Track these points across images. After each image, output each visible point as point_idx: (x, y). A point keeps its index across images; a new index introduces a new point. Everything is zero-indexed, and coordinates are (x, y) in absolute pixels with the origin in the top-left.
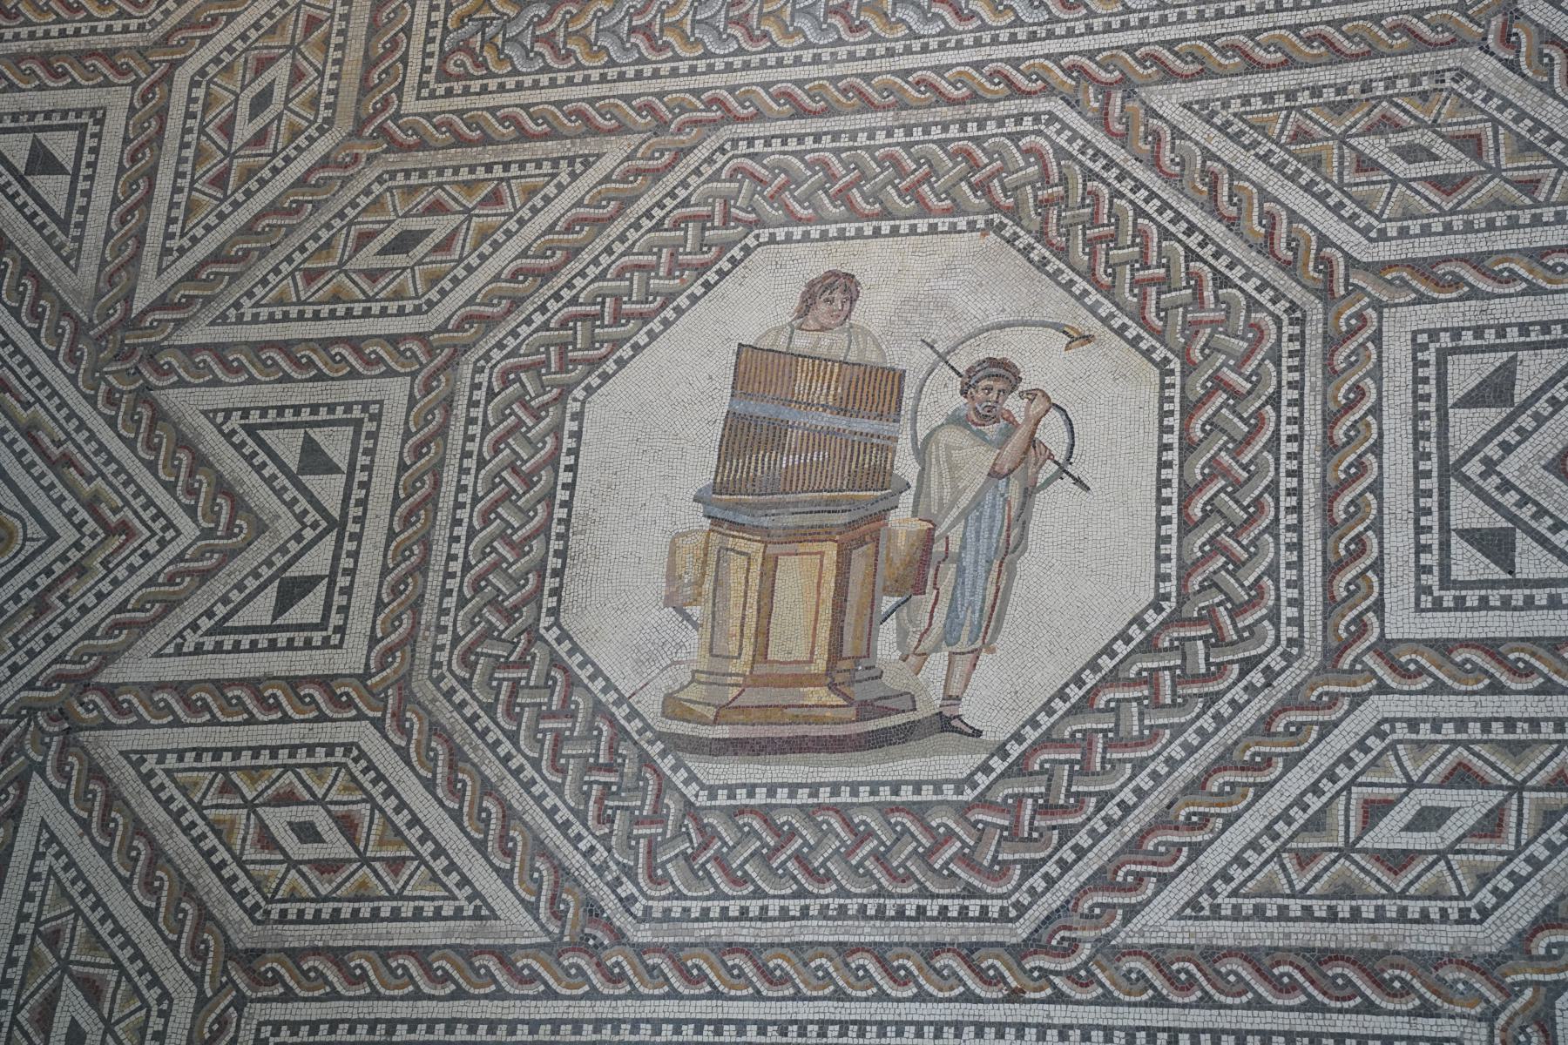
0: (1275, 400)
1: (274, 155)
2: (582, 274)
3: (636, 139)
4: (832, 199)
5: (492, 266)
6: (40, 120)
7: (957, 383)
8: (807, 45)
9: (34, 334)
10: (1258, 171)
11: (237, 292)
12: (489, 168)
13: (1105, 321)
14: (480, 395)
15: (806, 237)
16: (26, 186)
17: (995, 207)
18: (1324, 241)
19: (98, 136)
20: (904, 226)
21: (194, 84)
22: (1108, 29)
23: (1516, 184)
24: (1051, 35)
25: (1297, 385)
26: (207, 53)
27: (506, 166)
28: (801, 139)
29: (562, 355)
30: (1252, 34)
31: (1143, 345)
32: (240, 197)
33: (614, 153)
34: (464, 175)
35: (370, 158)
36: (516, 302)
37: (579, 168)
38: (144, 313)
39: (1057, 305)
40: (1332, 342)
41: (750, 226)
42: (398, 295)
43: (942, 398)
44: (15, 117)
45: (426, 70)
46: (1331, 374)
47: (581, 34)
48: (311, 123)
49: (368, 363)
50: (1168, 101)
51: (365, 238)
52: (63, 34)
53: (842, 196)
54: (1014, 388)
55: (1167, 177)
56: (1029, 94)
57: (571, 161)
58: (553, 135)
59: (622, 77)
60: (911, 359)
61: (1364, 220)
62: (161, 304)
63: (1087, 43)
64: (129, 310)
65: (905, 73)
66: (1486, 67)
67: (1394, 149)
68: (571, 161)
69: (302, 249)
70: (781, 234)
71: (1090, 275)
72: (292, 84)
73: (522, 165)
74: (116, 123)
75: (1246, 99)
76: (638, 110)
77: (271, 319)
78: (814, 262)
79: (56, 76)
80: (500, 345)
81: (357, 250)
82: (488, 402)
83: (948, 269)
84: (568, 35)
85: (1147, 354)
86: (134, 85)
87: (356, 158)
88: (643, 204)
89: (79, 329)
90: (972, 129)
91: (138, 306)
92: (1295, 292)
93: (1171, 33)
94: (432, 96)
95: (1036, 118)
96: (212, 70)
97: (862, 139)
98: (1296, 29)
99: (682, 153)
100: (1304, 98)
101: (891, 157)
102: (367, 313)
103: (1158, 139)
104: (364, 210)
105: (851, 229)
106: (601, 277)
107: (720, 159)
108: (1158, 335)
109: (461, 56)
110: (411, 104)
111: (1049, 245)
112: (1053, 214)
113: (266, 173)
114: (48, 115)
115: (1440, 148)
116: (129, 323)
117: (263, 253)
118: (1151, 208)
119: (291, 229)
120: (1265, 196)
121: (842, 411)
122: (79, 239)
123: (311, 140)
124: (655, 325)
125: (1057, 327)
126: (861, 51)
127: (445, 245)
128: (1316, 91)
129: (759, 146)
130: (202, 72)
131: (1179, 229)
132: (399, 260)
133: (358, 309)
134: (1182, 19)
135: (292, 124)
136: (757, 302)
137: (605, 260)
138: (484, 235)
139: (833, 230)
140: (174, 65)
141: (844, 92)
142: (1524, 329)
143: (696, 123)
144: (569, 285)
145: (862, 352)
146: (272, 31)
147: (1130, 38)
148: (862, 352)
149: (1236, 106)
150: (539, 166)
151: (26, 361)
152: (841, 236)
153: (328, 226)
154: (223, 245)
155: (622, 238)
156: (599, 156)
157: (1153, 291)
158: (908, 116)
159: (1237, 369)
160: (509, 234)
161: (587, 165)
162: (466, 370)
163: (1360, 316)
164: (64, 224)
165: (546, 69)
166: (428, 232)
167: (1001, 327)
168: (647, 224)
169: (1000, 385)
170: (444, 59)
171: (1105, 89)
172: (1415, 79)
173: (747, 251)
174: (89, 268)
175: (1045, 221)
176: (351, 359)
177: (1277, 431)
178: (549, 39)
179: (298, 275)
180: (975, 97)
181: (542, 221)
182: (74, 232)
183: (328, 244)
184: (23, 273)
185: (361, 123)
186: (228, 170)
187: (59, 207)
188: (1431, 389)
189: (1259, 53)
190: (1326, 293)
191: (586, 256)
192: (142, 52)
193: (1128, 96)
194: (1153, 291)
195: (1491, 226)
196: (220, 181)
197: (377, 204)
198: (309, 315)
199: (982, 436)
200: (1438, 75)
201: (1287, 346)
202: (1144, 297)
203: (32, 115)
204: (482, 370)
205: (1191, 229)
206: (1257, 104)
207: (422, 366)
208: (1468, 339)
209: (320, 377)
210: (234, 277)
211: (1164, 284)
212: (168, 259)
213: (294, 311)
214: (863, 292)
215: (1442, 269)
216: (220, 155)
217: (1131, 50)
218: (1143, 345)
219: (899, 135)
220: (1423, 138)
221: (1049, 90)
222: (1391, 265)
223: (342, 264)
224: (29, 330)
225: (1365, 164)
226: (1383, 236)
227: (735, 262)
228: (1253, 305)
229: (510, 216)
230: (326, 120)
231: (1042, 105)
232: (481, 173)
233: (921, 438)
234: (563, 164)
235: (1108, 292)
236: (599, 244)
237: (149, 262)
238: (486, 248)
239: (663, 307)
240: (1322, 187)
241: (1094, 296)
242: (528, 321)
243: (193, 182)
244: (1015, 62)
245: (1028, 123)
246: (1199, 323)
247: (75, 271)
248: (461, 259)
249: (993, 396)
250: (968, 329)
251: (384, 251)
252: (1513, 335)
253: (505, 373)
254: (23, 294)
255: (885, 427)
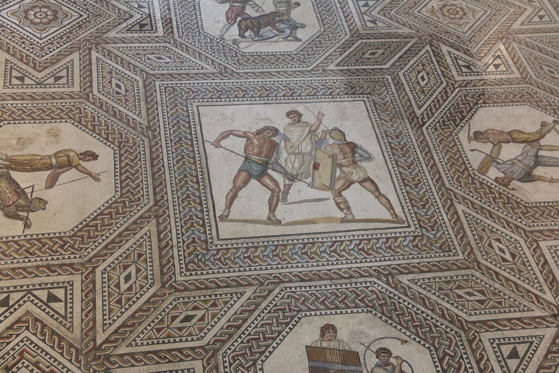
0: (461, 357)
1: (136, 293)
2: (250, 326)
3: (255, 287)
4: (320, 304)
5: (220, 325)
6: (49, 286)
7: (374, 355)
8: (298, 262)
9: (62, 354)
10: (434, 297)
11: (133, 336)
12: (210, 296)
13: (409, 336)
14: (227, 364)
15: (316, 315)
16: (48, 306)
17: (367, 306)
18: (458, 316)
19: (72, 289)
20: (344, 311)
21: (103, 273)
22: (381, 261)
23: (496, 302)
24: (366, 262)
25: (466, 353)
26: (105, 264)
27: (216, 295)
28: (305, 287)
29: (250, 351)
30: (419, 263)
31: (422, 343)
32: (127, 306)
33: (249, 292)
34: (202, 298)
35: (170, 294)
36: (231, 336)
37: (239, 296)
38: (101, 345)
39: (394, 333)
40: (470, 342)
41: (298, 312)
42: (190, 335)
43: (371, 360)
44: (40, 285)
45: (181, 268)
46: (473, 351)
47: (229, 258)
48: (147, 284)
49: (186, 356)
50: (404, 279)
51: (174, 318)
52: (53, 259)
53: (322, 303)
54: (391, 356)
55: (411, 299)
56: (366, 276)
57: (236, 294)
58: (228, 286)
59: (245, 270)
60: (360, 349)
61: (465, 310)
62: (107, 341)
63: (377, 264)
64: (95, 344)
65: (330, 270)
66: (478, 274)
67: (465, 293)
68: (236, 294)
69: (153, 322)
70: (308, 314)
71: (400, 324)
72: (137, 273)
73: (221, 295)
74: (77, 286)
75: (423, 279)
76: (253, 279)
77: (148, 344)
78: (322, 321)
79: (53, 272)
80: (229, 349)
81: (172, 321)
82: (230, 367)
83: (360, 323)
84: (225, 259)
85: (424, 345)
86: (82, 274)
87: (165, 294)
88: (263, 306)
89: (77, 350)
90: (354, 285)
91: (98, 342)
92: (455, 329)
93: (398, 262)
94: (185, 275)
95: (371, 282)
96: (108, 269)
97: (323, 287)
98: (429, 263)
99: (270, 291)
100: (437, 280)
101: (333, 292)
102: (181, 341)
103: (405, 289)
104: (172, 309)
105: (328, 312)
106: (256, 327)
107: (283, 293)
108: (425, 340)
109: (192, 264)
110: (179, 278)
111: (386, 316)
112: (384, 308)
113: (135, 299)
114: (52, 284)
115: (475, 293)
116: (96, 348)
117: (140, 324)
118: (410, 306)
119: (148, 316)
120: (438, 304)
121: (343, 364)
122: (72, 322)
123: (148, 289)
124: (278, 341)
125: (397, 339)
126: (315, 264)
127: (202, 319)
128: (440, 278)
129: (293, 289)
130: (105, 269)
131: (419, 312)
132: (187, 324)
133: (178, 339)
134: (399, 259)
135: (140, 285)
136: (307, 332)
137: (256, 322)
138: (214, 316)
139: (323, 312)
140: (95, 268)
141: (314, 275)
142: (514, 338)
143: (272, 283)
144: (246, 330)
145: (343, 347)
146: (127, 257)
147: (388, 263)
148: (343, 347)
149: (421, 281)
150: (226, 295)
151: (60, 363)
152: (326, 314)
153: (160, 314)
154: (125, 322)
155: (259, 315)
156: (245, 292)
157: (419, 328)
158: (336, 282)
159: (449, 349)
160: (222, 315)
161: (242, 295)
162: (220, 357)
163: (473, 335)
164: (65, 318)
165: (220, 268)
166: (195, 315)
167: (382, 338)
168: (266, 312)
169: (386, 355)
170: (186, 265)
171: (386, 276)
172: (463, 276)
173: (300, 319)
174: (77, 332)
175: (383, 310)
176: (179, 355)
177: (466, 366)
178: (219, 259)
179: (154, 330)
180: (351, 277)
181: (232, 311)
182: (69, 320)
183: (162, 320)
184: (53, 334)
185: (164, 284)
186: (121, 299)
187: (62, 312)
188: (499, 354)
189: (422, 268)
190: (463, 329)
191: (249, 321)
192: (82, 264)
193: (393, 278)
194: (419, 328)
195: (495, 313)
196: (119, 302)
197: (175, 307)
198: (161, 342)
199: (387, 370)
200: (467, 275)
201: (459, 343)
202: (417, 330)
203: (46, 284)
204: (225, 357)
205: (423, 312)
206: (427, 281)
207: (205, 357)
208: (502, 341)
209: (170, 362)
210: (131, 332)
211: (421, 326)
212: (105, 327)
213: (155, 341)
214: (338, 330)
215: (489, 323)
216: (117, 294)
217: (389, 266)
218: (422, 343)
219: (333, 287)
220: (471, 291)
221: (371, 276)
222: (476, 322)
223: (168, 326)
224: (59, 353)
225: (459, 297)
226: (471, 315)
227: (297, 322)
228: (446, 332)
229: (221, 310)
230: (151, 283)
231: (370, 279)
232: (208, 298)
233: (369, 370)
234: (234, 295)
235: (407, 328)
236: (252, 318)
237: (99, 328)
238: (216, 319)
239: (279, 335)
240: (451, 302)
241: (404, 330)
242: (236, 341)
243: (109, 303)
244: (360, 268)
245: (368, 284)
246: (434, 337)
247: (72, 332)
248: (208, 323)
249: (386, 358)
250: (372, 340)
251: (182, 321)
252: (512, 340)
253: (233, 357)
254: (54, 341)
255: (358, 369)
